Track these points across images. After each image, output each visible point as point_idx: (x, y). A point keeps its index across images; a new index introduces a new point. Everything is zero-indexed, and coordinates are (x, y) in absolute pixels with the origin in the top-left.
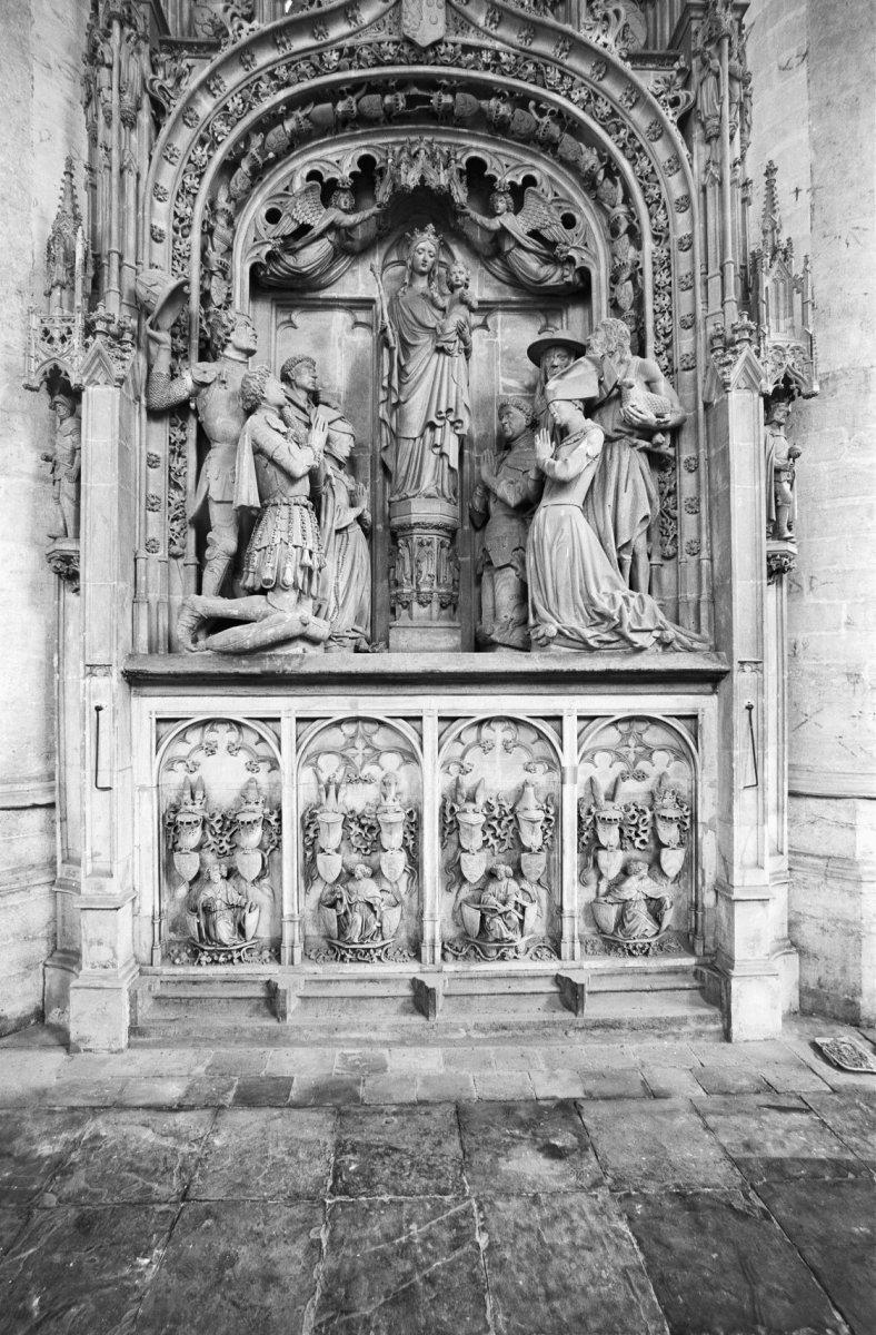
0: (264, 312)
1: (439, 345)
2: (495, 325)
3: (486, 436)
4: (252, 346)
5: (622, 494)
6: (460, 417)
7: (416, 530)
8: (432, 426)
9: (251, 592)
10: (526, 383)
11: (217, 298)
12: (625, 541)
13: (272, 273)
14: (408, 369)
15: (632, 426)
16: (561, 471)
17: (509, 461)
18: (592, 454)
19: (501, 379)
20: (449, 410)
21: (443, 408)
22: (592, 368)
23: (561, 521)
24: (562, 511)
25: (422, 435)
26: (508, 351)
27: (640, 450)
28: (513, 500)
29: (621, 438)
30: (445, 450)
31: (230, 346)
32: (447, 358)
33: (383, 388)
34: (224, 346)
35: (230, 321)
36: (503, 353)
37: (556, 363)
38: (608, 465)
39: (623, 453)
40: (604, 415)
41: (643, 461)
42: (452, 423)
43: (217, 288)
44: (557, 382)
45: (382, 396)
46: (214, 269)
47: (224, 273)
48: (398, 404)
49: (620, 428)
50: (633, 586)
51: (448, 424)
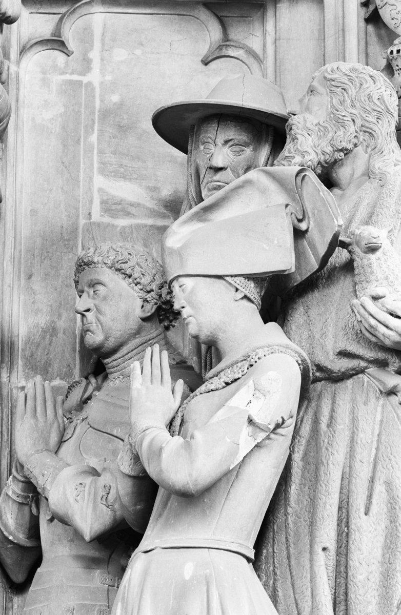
2: (86, 36)
3: (51, 331)
5: (359, 520)
10: (166, 192)
15: (383, 348)
16: (177, 468)
17: (94, 410)
18: (266, 418)
19: (99, 181)
22: (279, 197)
23: (183, 591)
24: (189, 566)
26: (121, 105)
28: (91, 520)
29: (362, 371)
36: (105, 114)
37: (218, 162)
38: (324, 440)
39: (362, 411)
40: (313, 312)
44: (197, 226)
49: (353, 348)
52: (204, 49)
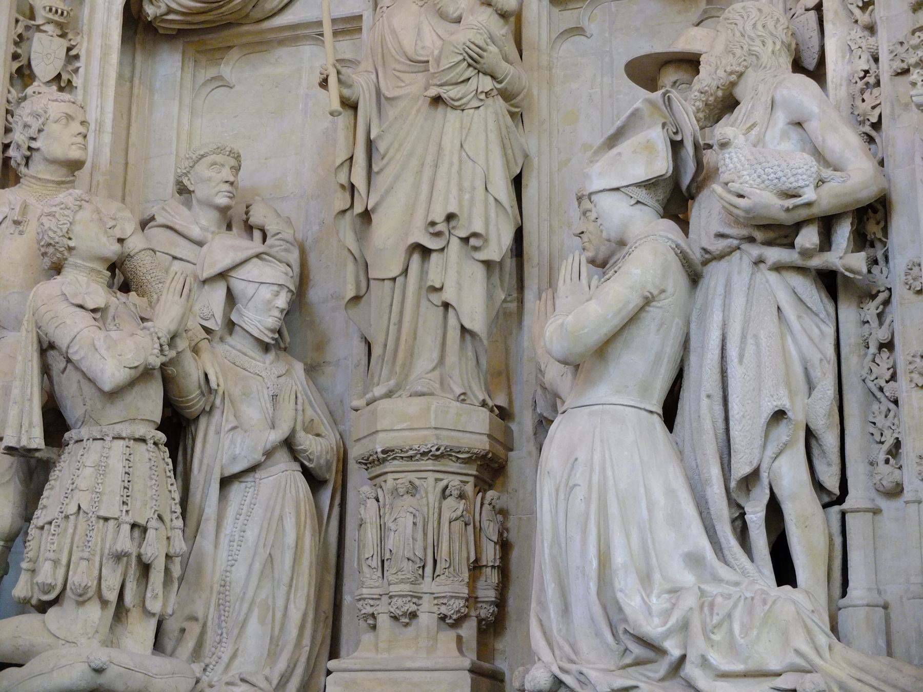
0: (169, 65)
1: (433, 92)
4: (75, 154)
6: (478, 227)
7: (389, 467)
8: (425, 252)
9: (24, 606)
11: (44, 68)
12: (747, 470)
13: (170, 11)
14: (382, 146)
20: (450, 217)
21: (439, 215)
25: (405, 272)
27: (778, 268)
30: (448, 295)
31: (36, 156)
32: (453, 117)
33: (343, 186)
34: (28, 159)
35: (37, 116)
41: (781, 288)
42: (465, 240)
43: (46, 54)
45: (341, 201)
46: (39, 21)
47: (59, 25)
48: (366, 216)
50: (785, 573)
51: (455, 243)
52: (695, 18)
